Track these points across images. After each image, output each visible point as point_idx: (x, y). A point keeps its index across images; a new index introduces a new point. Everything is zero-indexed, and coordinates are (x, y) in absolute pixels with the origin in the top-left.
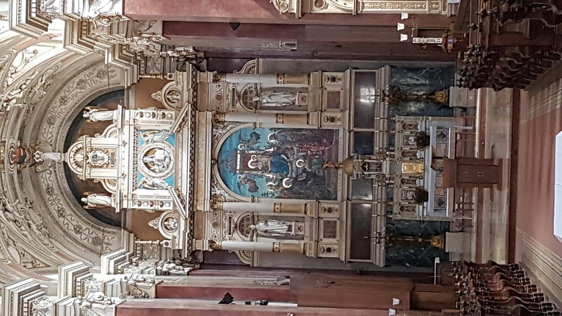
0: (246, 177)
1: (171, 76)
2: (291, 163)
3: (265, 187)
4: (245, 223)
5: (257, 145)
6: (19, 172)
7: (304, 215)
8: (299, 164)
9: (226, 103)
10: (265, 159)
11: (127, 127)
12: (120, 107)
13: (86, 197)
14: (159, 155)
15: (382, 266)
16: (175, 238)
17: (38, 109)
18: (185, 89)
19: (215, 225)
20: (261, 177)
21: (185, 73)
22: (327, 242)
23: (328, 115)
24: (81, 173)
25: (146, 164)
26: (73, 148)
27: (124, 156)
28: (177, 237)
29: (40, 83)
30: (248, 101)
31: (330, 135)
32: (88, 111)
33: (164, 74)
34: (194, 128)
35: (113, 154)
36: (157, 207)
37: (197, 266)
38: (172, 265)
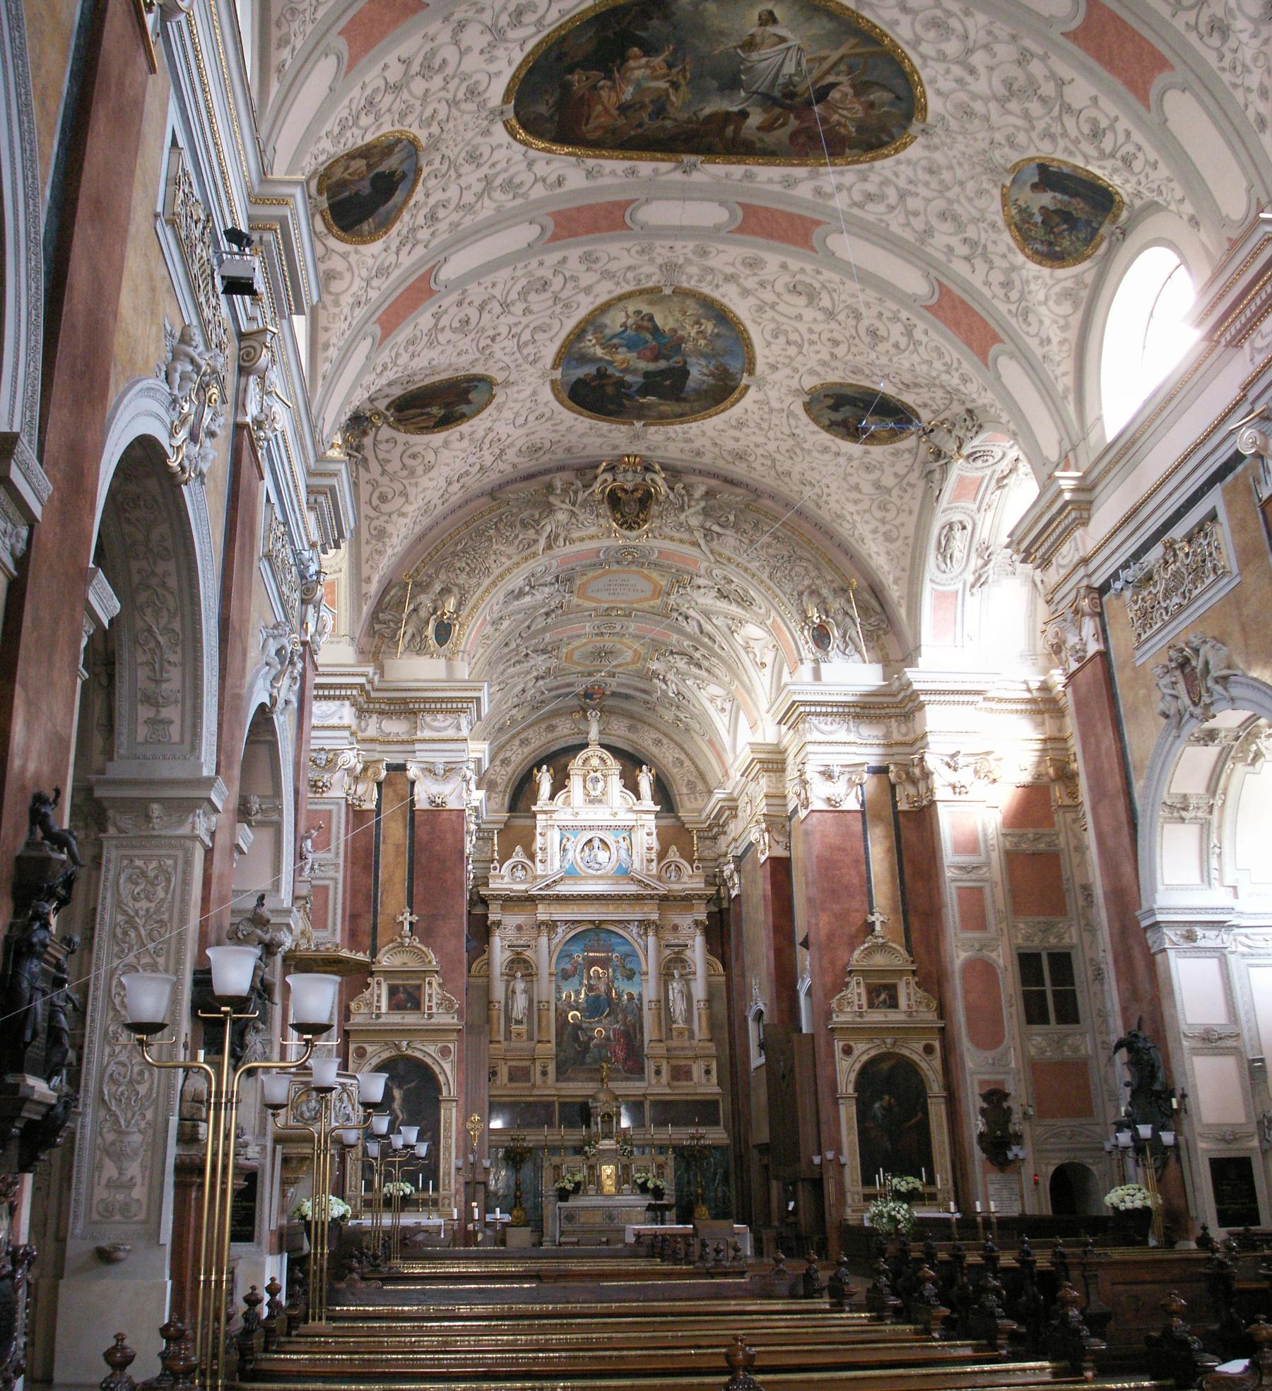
10: (603, 988)
11: (634, 816)
12: (658, 808)
14: (602, 856)
19: (519, 928)
20: (581, 984)
24: (576, 765)
26: (607, 755)
27: (598, 815)
28: (504, 880)
29: (682, 716)
34: (638, 898)
35: (600, 801)
36: (539, 856)
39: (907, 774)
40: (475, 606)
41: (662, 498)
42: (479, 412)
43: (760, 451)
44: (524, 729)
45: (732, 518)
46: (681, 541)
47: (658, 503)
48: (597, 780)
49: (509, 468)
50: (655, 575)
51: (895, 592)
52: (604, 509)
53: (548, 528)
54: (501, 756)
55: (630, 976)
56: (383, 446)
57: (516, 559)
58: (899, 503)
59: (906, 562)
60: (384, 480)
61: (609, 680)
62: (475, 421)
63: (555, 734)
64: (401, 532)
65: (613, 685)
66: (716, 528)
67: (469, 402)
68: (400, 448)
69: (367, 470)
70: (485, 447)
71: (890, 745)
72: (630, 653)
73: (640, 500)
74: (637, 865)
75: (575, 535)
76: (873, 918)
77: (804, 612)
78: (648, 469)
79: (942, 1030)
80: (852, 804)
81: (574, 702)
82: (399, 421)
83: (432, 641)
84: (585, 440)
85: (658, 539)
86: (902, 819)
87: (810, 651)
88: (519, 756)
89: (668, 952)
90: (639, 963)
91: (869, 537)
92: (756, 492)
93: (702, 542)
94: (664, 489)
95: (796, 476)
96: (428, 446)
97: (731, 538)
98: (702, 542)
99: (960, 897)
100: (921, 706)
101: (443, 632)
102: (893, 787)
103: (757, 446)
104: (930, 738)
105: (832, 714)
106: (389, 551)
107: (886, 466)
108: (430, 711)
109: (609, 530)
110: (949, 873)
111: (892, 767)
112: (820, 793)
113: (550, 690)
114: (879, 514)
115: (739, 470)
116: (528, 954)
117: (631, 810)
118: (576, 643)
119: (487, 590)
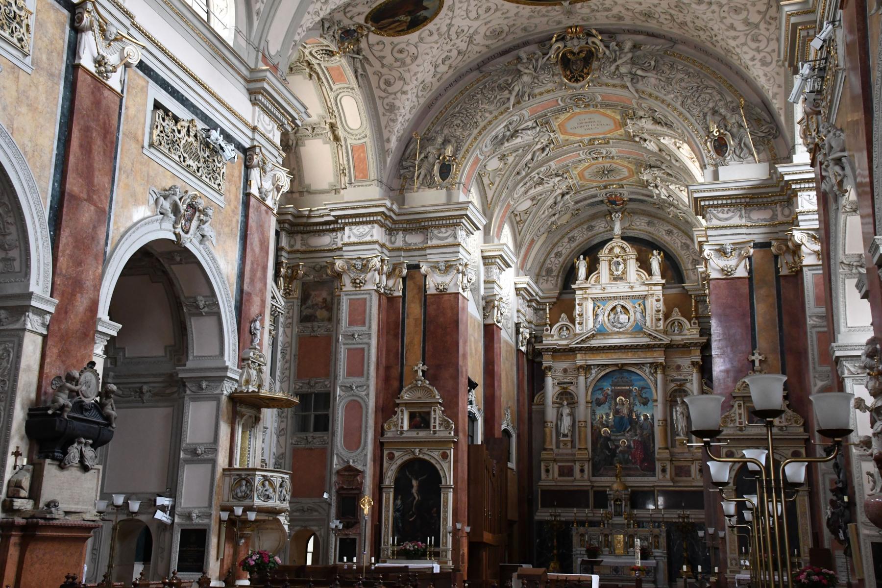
0: (608, 395)
1: (694, 323)
2: (624, 435)
3: (602, 412)
4: (569, 396)
5: (638, 403)
6: (602, 201)
7: (577, 446)
8: (623, 441)
9: (675, 375)
10: (625, 411)
11: (647, 288)
12: (664, 281)
13: (584, 259)
14: (623, 318)
15: (536, 518)
16: (553, 336)
17: (660, 212)
18: (684, 337)
19: (565, 371)
20: (610, 408)
21: (698, 336)
22: (555, 469)
23: (668, 467)
25: (614, 308)
26: (625, 244)
27: (621, 288)
28: (554, 338)
30: (677, 394)
31: (652, 471)
32: (659, 254)
33: (697, 318)
34: (648, 347)
35: (621, 279)
36: (578, 320)
37: (530, 357)
38: (528, 336)
39: (787, 246)
40: (467, 151)
41: (600, 55)
42: (436, 14)
43: (659, 10)
44: (571, 231)
45: (653, 63)
46: (614, 86)
47: (598, 59)
48: (618, 264)
49: (485, 50)
50: (609, 112)
51: (777, 104)
52: (558, 69)
53: (516, 89)
54: (555, 251)
55: (645, 403)
56: (376, 48)
57: (495, 113)
58: (767, 34)
59: (781, 80)
60: (384, 71)
61: (621, 190)
62: (437, 20)
63: (594, 232)
64: (407, 106)
65: (626, 194)
66: (639, 72)
67: (426, 8)
68: (389, 48)
69: (371, 65)
70: (454, 37)
71: (774, 226)
72: (625, 170)
73: (584, 58)
74: (648, 323)
75: (537, 91)
76: (753, 358)
77: (708, 128)
78: (589, 35)
79: (807, 441)
80: (741, 272)
81: (604, 208)
82: (380, 29)
83: (437, 178)
84: (536, 21)
85: (597, 86)
86: (782, 282)
87: (711, 158)
88: (565, 248)
89: (673, 385)
90: (652, 393)
91: (750, 63)
92: (671, 40)
93: (629, 84)
94: (602, 47)
95: (691, 25)
96: (408, 44)
97: (652, 79)
98: (629, 84)
99: (819, 339)
100: (795, 193)
101: (445, 171)
102: (776, 257)
103: (655, 6)
104: (800, 218)
105: (727, 205)
106: (400, 119)
107: (748, 6)
108: (436, 227)
109: (562, 84)
110: (810, 322)
111: (774, 243)
112: (715, 266)
113: (576, 203)
114: (754, 45)
115: (652, 25)
116: (572, 388)
117: (644, 284)
118: (581, 167)
119: (475, 138)
